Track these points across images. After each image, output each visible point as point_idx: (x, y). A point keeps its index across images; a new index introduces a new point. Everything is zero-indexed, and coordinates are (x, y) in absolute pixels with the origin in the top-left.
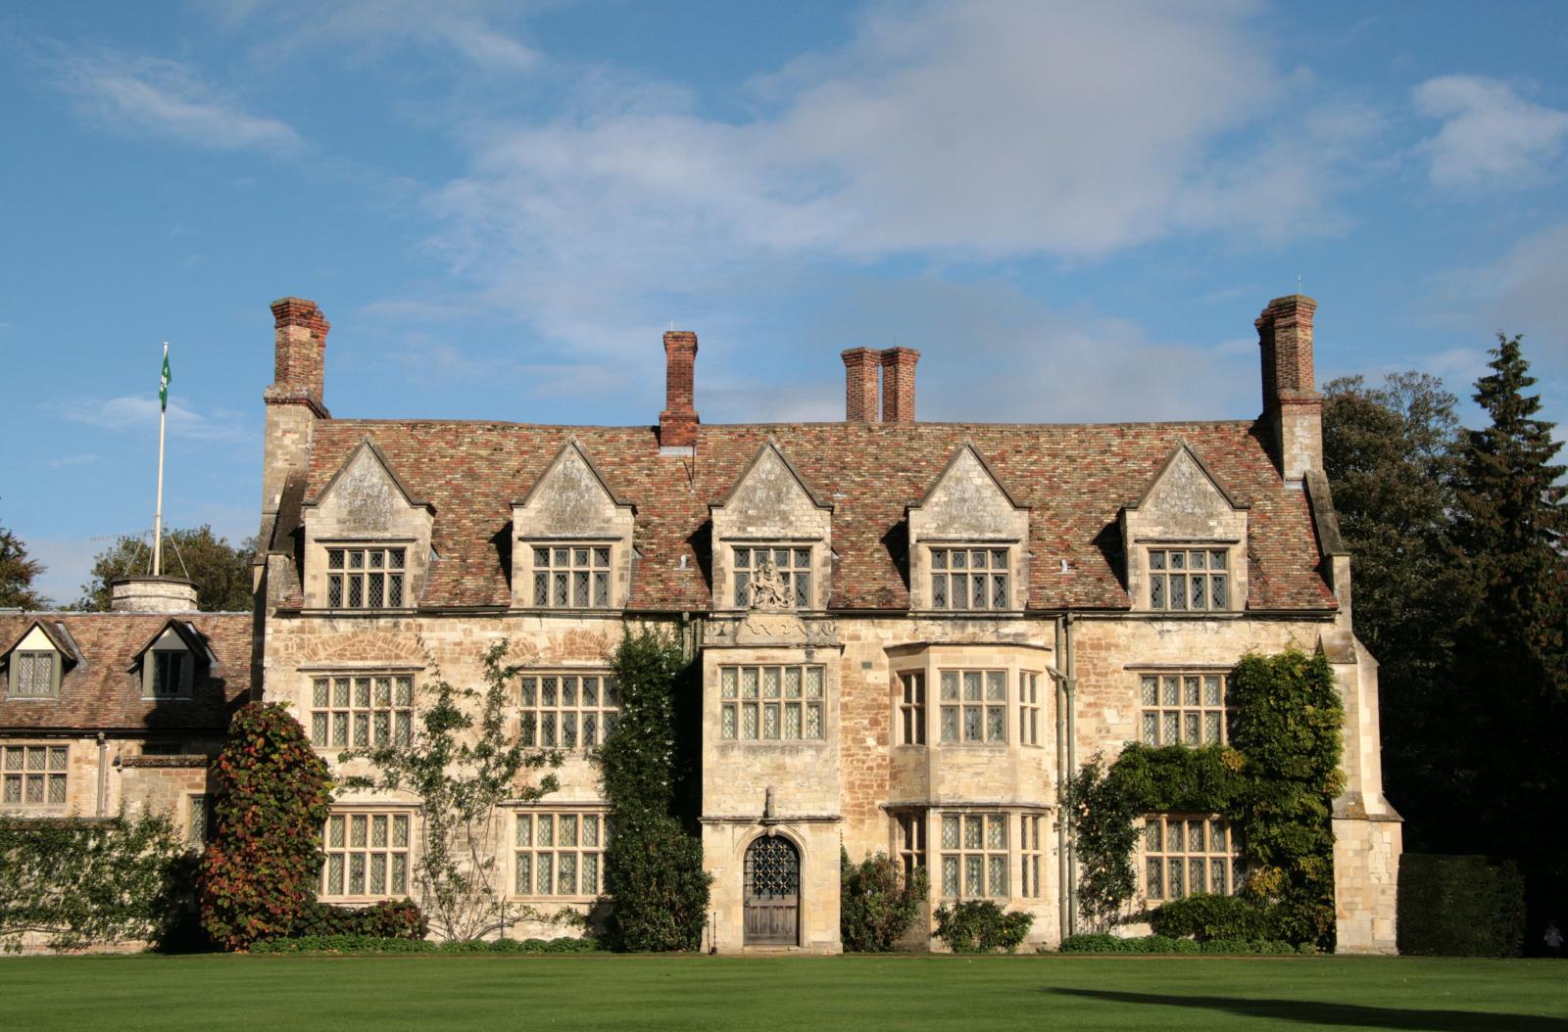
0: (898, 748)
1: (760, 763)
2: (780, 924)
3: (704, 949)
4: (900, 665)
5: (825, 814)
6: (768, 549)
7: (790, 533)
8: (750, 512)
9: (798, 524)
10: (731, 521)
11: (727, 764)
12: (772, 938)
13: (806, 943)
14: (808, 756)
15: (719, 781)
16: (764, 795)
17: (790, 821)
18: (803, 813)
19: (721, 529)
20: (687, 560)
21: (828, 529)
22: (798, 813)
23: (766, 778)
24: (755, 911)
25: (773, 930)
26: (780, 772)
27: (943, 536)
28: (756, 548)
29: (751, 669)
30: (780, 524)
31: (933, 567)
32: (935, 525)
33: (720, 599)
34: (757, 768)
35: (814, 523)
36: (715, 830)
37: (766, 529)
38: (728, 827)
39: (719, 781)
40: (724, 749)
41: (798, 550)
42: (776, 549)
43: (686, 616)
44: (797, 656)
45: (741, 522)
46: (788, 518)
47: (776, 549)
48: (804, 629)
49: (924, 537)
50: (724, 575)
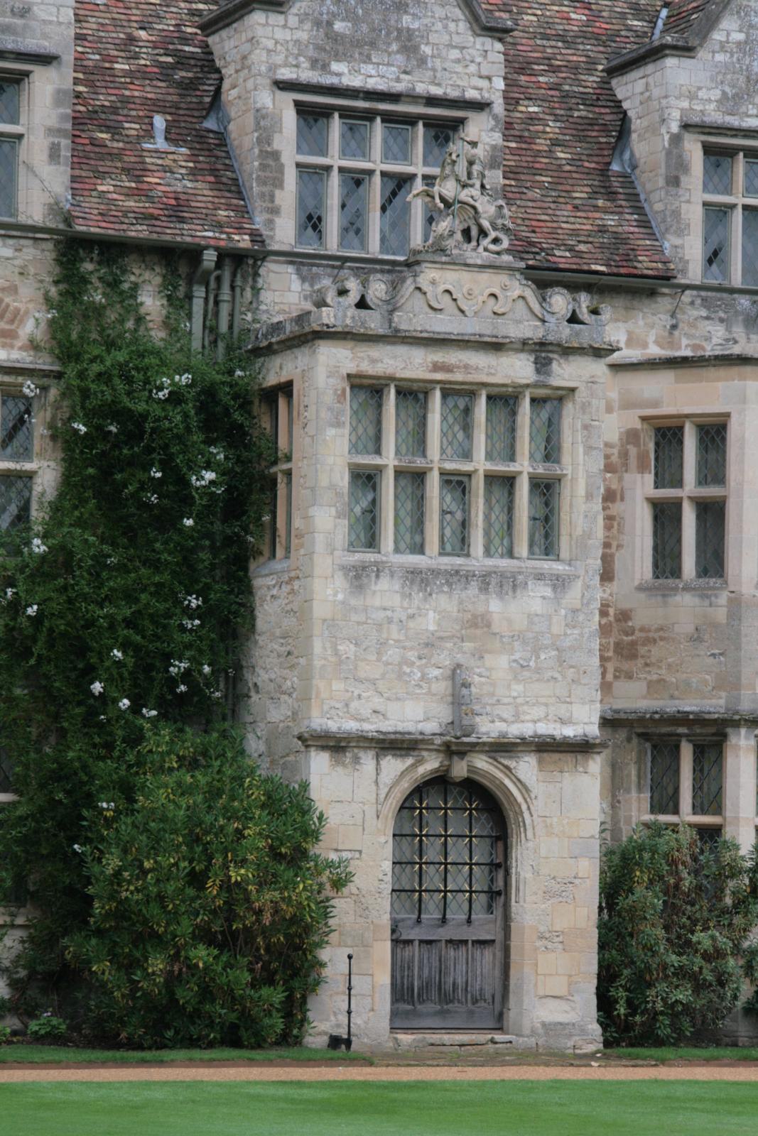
0: (640, 588)
1: (436, 612)
2: (460, 981)
3: (316, 1039)
4: (656, 404)
5: (569, 732)
6: (369, 116)
7: (421, 88)
8: (339, 26)
9: (438, 63)
10: (297, 42)
11: (365, 610)
12: (442, 1013)
13: (527, 1031)
14: (535, 599)
15: (347, 649)
16: (442, 687)
17: (503, 748)
18: (526, 729)
19: (279, 59)
20: (167, 131)
21: (500, 84)
22: (515, 730)
23: (449, 645)
24: (408, 951)
25: (446, 997)
26: (479, 632)
27: (734, 121)
28: (346, 113)
29: (413, 394)
30: (400, 59)
31: (706, 189)
32: (715, 95)
33: (270, 222)
34: (430, 622)
35: (467, 65)
36: (338, 763)
37: (370, 69)
38: (368, 760)
39: (347, 649)
40: (359, 576)
41: (430, 122)
42: (388, 118)
43: (210, 257)
44: (518, 369)
45: (319, 48)
46: (416, 49)
47: (388, 118)
48: (536, 307)
49: (696, 119)
50: (281, 169)
